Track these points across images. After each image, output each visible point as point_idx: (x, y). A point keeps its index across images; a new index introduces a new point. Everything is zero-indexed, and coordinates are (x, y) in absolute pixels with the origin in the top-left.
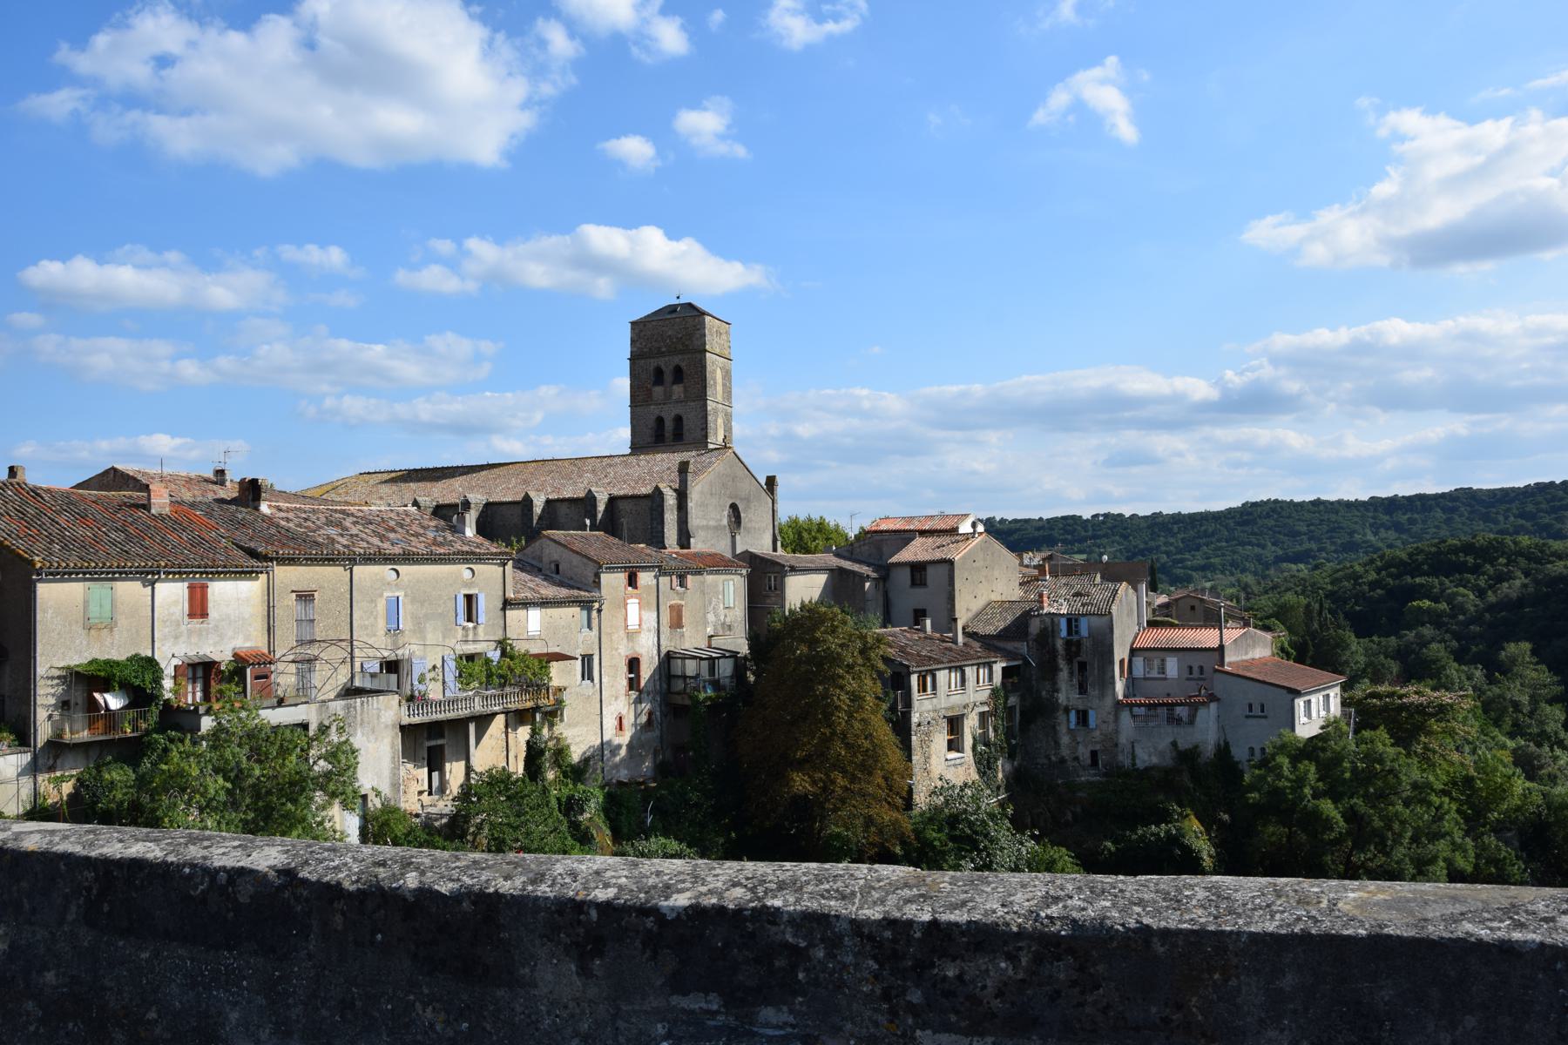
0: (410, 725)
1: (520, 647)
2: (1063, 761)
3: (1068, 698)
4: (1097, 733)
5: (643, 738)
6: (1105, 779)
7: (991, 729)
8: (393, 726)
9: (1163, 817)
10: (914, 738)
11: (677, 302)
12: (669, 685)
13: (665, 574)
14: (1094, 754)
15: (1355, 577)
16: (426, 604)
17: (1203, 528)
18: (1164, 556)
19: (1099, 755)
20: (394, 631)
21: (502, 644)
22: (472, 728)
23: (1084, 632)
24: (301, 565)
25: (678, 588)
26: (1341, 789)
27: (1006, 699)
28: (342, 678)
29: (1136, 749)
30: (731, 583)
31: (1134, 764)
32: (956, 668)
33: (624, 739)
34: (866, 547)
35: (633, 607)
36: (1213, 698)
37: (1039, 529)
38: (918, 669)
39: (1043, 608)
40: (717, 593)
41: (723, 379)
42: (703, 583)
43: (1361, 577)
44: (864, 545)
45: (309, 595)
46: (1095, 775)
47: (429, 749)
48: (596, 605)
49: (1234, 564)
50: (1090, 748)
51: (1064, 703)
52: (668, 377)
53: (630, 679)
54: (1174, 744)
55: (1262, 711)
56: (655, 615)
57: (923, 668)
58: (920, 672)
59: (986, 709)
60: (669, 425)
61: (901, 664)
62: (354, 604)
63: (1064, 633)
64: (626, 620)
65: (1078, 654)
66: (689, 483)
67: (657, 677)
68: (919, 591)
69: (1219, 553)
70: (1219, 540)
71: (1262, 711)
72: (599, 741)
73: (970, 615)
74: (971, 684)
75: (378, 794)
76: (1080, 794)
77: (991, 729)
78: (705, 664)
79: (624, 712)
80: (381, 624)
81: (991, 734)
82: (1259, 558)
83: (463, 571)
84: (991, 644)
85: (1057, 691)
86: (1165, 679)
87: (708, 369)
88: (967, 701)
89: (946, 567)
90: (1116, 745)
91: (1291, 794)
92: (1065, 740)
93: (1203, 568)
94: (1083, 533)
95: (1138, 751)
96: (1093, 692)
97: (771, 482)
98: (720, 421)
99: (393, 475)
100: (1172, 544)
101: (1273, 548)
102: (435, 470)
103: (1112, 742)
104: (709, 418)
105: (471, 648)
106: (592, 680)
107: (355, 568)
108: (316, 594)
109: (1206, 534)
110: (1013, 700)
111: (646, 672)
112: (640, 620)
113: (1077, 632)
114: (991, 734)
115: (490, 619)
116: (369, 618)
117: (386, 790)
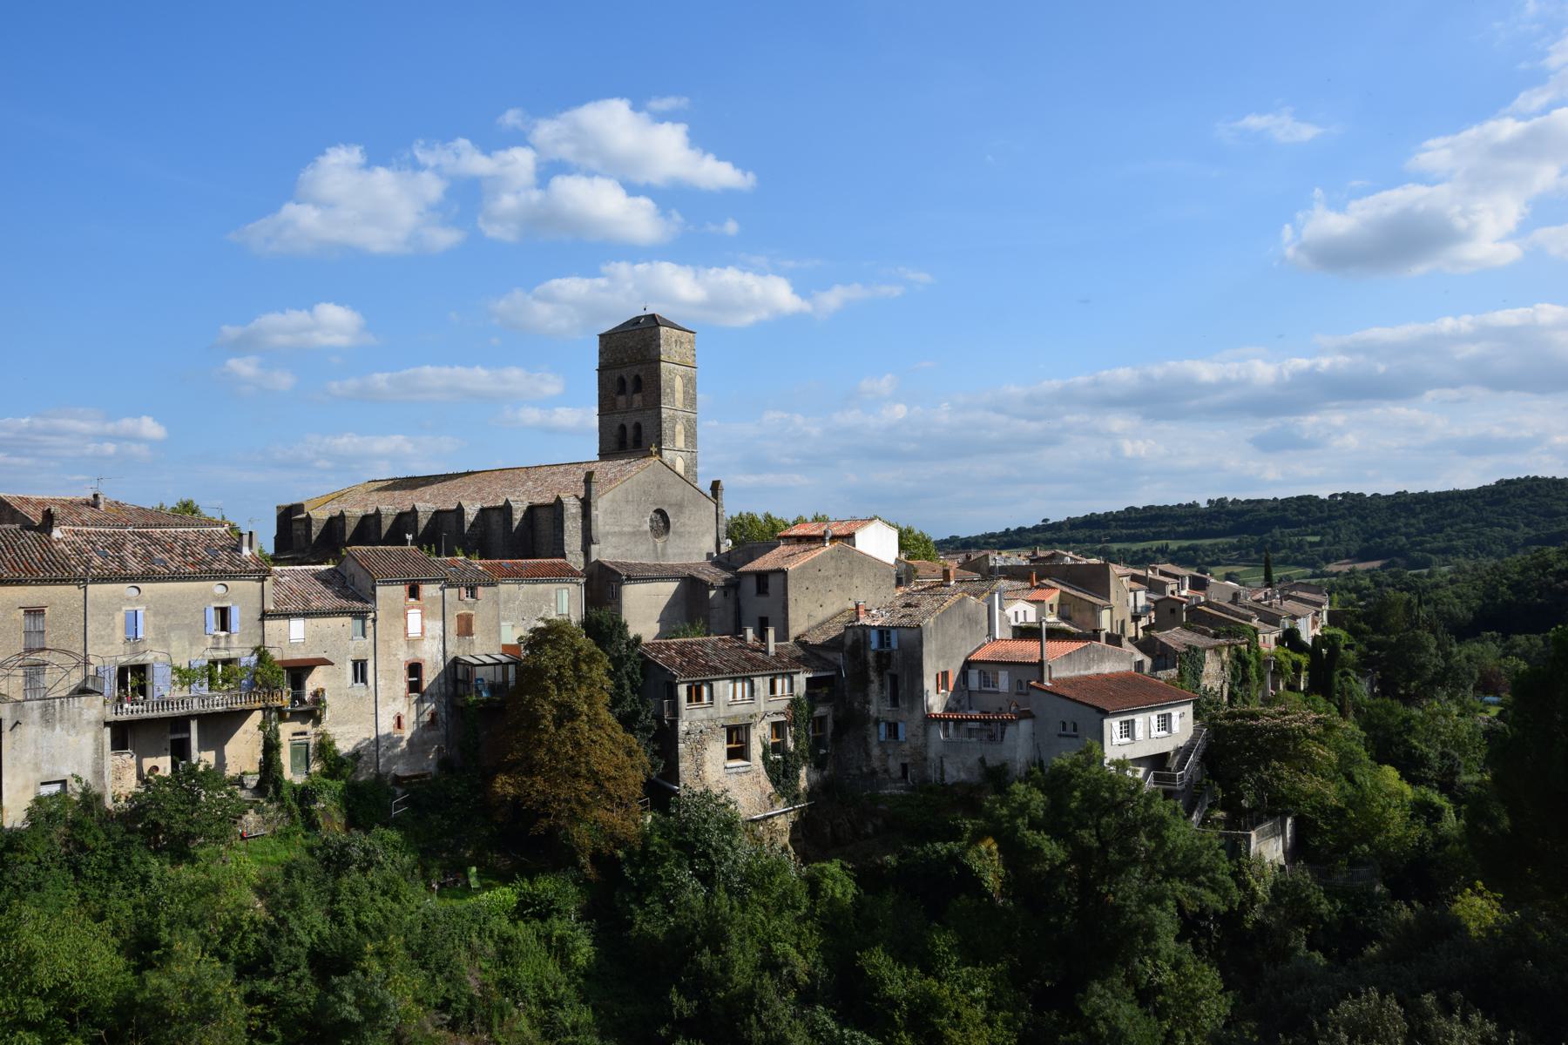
0: (116, 722)
1: (276, 654)
2: (874, 772)
3: (879, 711)
4: (907, 746)
5: (425, 736)
6: (908, 793)
7: (789, 739)
8: (97, 722)
9: (954, 834)
10: (681, 746)
11: (644, 313)
12: (456, 689)
13: (451, 586)
14: (904, 767)
15: (1546, 565)
16: (171, 617)
17: (1448, 508)
18: (1404, 539)
19: (909, 768)
20: (133, 638)
21: (261, 654)
22: (194, 725)
23: (894, 645)
24: (30, 584)
25: (470, 600)
26: (1065, 819)
27: (812, 709)
28: (76, 678)
29: (945, 764)
30: (565, 591)
31: (943, 779)
32: (743, 679)
33: (407, 733)
34: (740, 555)
35: (414, 619)
36: (1028, 715)
37: (1271, 510)
38: (687, 679)
39: (858, 620)
40: (549, 601)
41: (685, 386)
42: (497, 594)
43: (1552, 566)
44: (739, 552)
45: (39, 611)
46: (902, 788)
47: (172, 741)
48: (372, 615)
49: (1480, 547)
50: (900, 761)
51: (875, 715)
52: (630, 387)
53: (410, 682)
54: (982, 761)
55: (1075, 730)
56: (440, 624)
57: (694, 679)
58: (693, 682)
59: (782, 718)
60: (630, 432)
61: (672, 674)
62: (88, 617)
63: (874, 645)
64: (406, 628)
65: (888, 666)
66: (593, 492)
67: (442, 681)
68: (762, 599)
69: (1463, 535)
70: (1465, 522)
71: (1075, 730)
72: (373, 737)
73: (813, 623)
74: (762, 695)
75: (79, 780)
76: (881, 807)
77: (789, 739)
78: (499, 668)
79: (404, 712)
80: (120, 635)
81: (791, 745)
82: (1508, 540)
83: (216, 588)
84: (809, 654)
85: (869, 702)
86: (998, 693)
87: (663, 377)
88: (756, 711)
89: (780, 577)
90: (925, 759)
91: (1008, 822)
92: (876, 751)
93: (1444, 551)
94: (1319, 515)
95: (947, 766)
96: (903, 705)
97: (715, 486)
98: (679, 428)
99: (385, 484)
100: (1412, 525)
101: (1527, 530)
102: (436, 477)
103: (921, 756)
104: (664, 425)
105: (223, 655)
106: (366, 683)
107: (89, 586)
108: (46, 610)
109: (1451, 515)
110: (820, 711)
111: (428, 677)
112: (423, 628)
113: (889, 645)
114: (791, 745)
115: (245, 629)
116: (105, 629)
117: (87, 775)
